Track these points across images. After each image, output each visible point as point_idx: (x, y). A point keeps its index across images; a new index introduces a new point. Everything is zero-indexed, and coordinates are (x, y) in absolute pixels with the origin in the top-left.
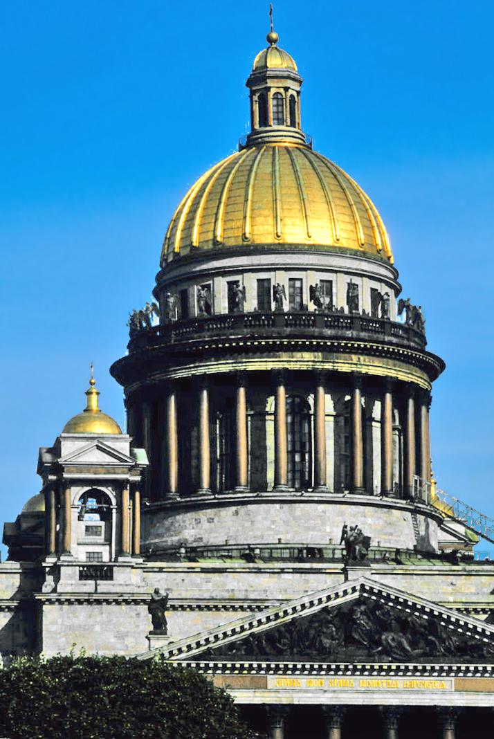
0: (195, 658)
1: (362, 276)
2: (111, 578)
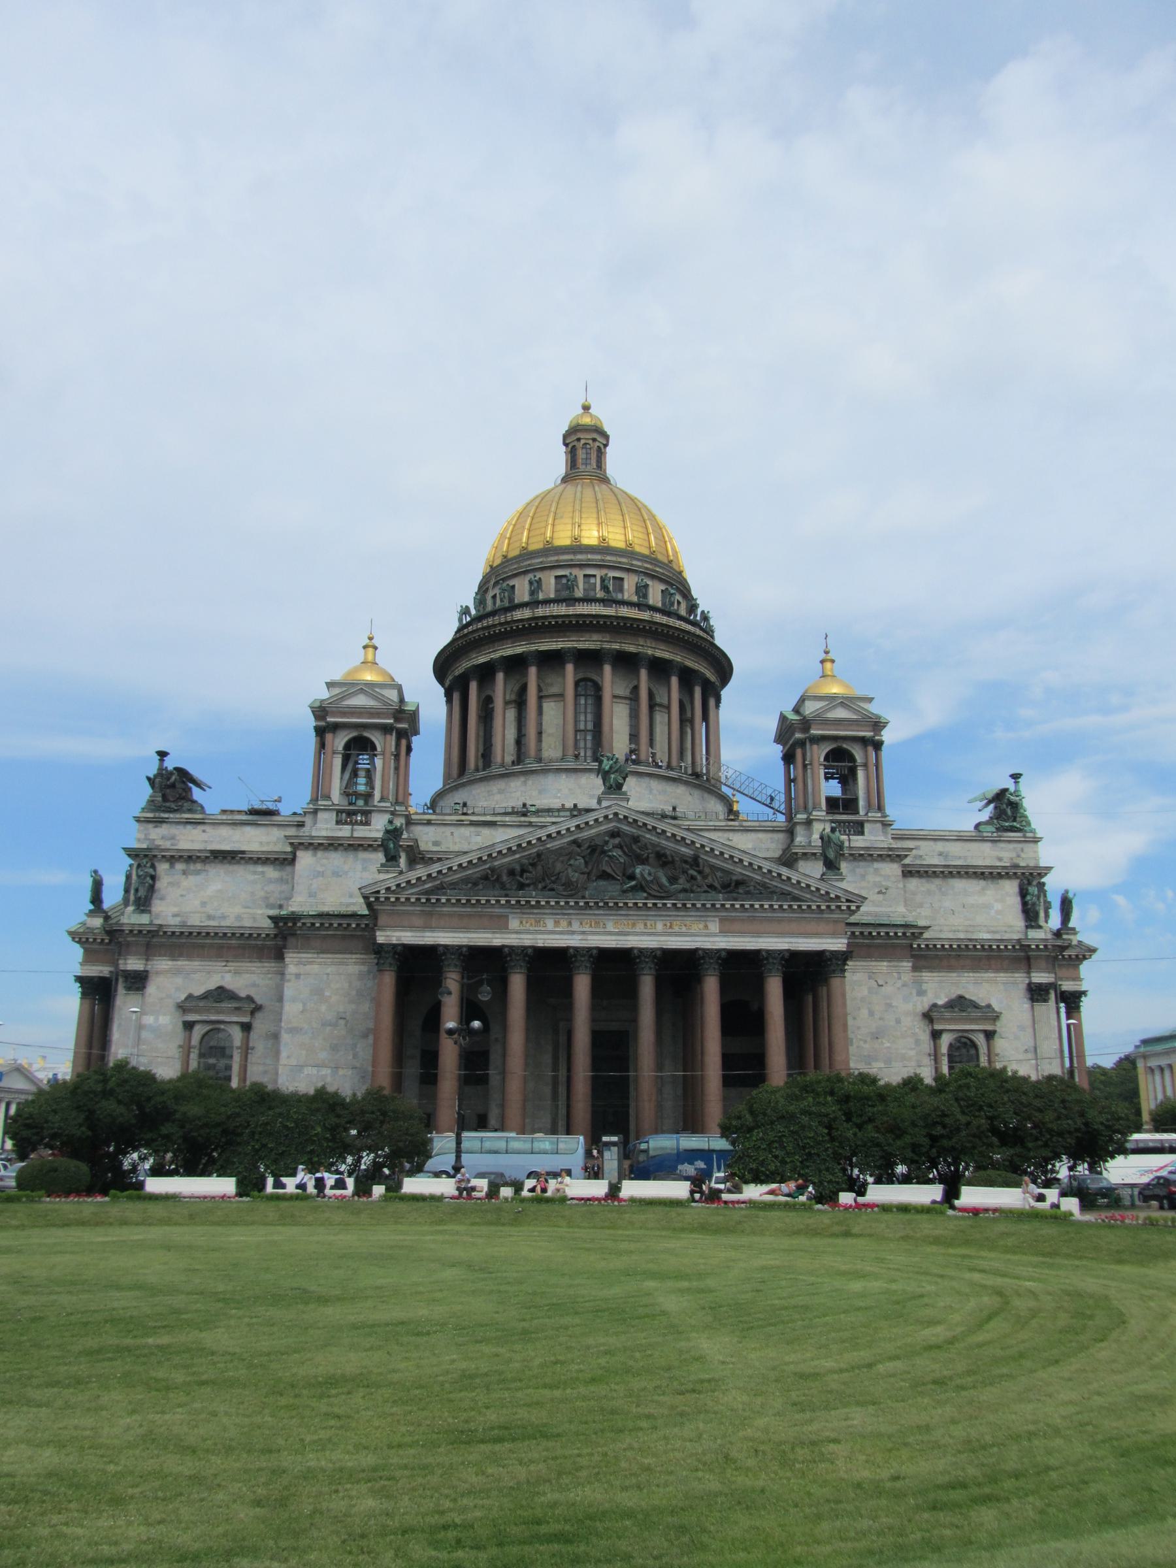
0: (427, 892)
1: (653, 577)
2: (367, 823)
